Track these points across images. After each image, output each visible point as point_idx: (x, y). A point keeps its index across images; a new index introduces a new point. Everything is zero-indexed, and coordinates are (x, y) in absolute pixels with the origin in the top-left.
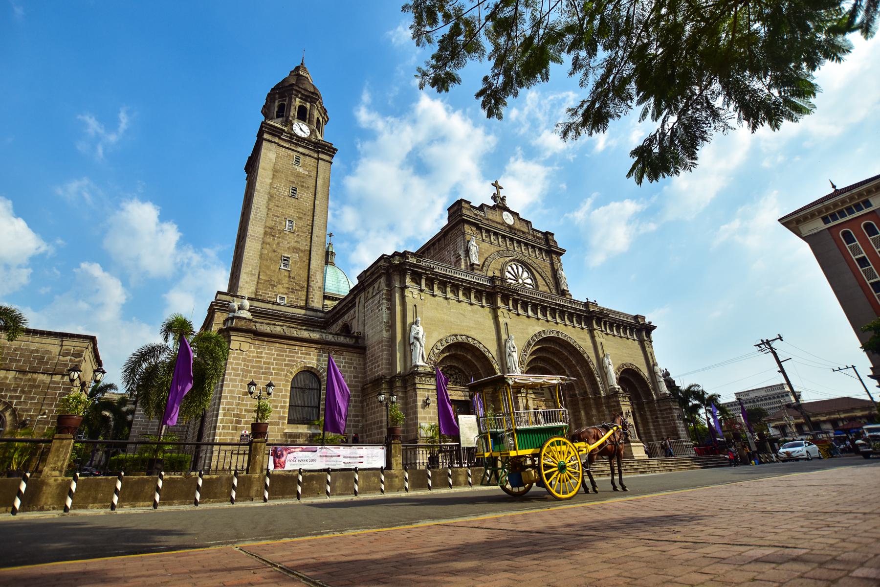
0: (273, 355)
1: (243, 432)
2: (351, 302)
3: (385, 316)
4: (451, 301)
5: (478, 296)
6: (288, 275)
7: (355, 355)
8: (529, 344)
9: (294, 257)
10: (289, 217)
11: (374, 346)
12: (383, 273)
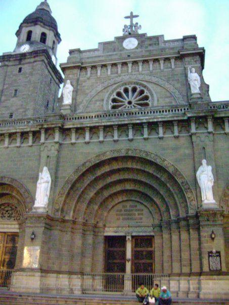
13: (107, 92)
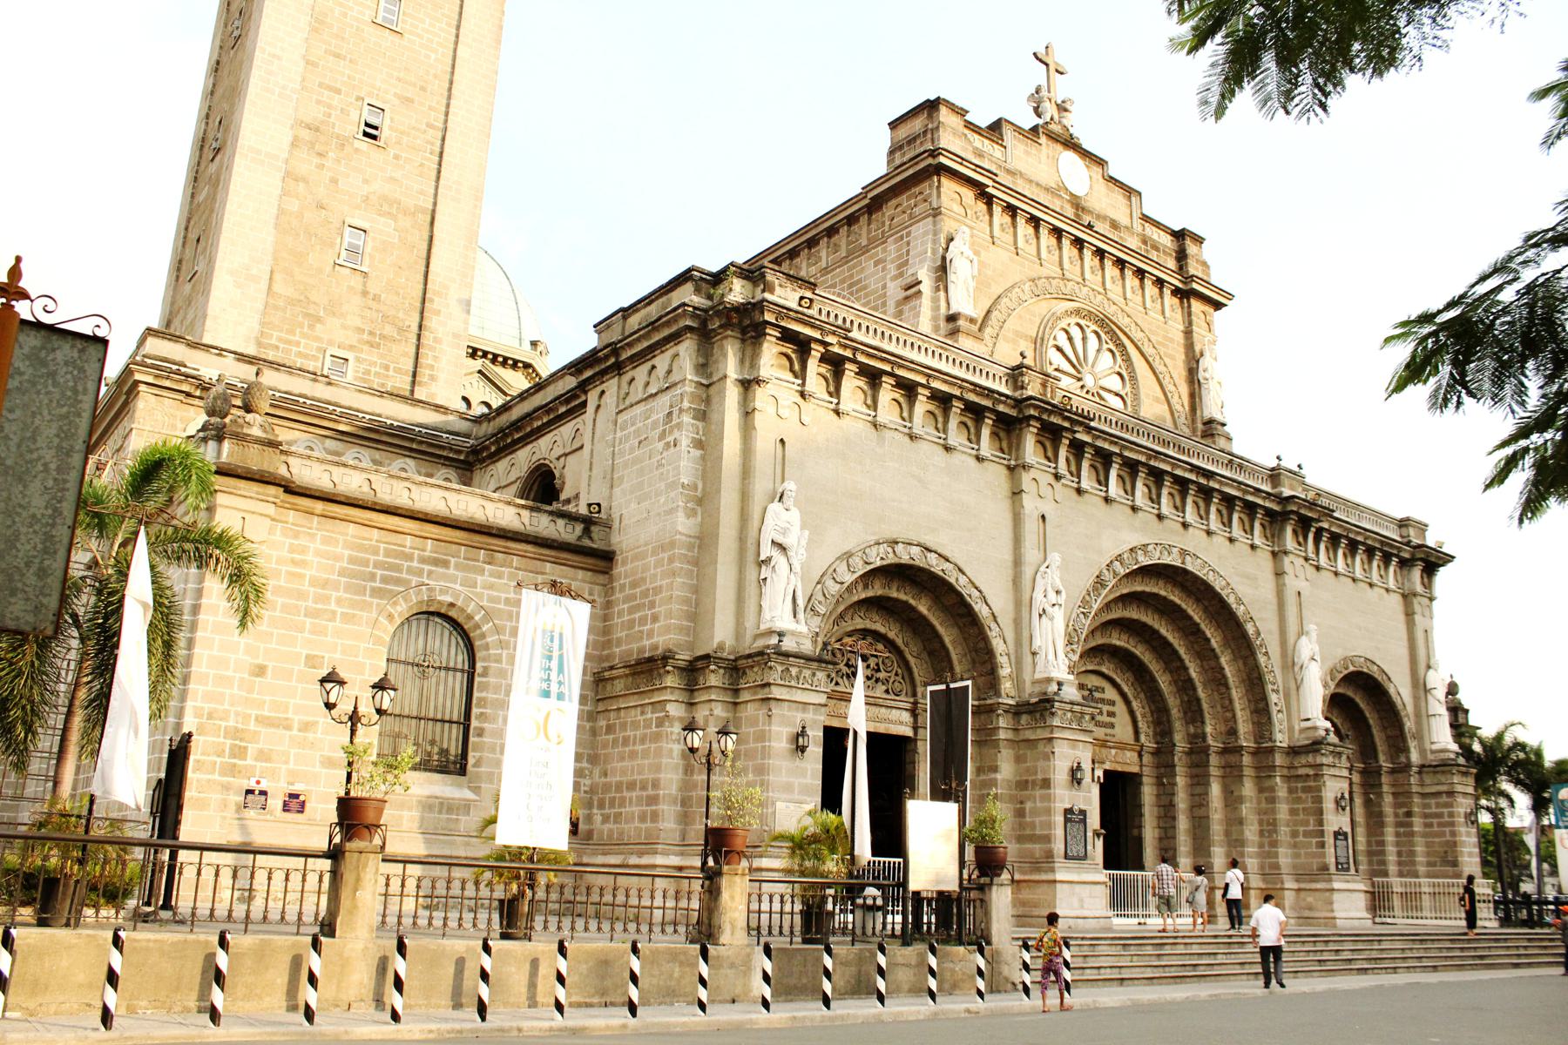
0: (337, 558)
2: (567, 401)
3: (686, 463)
5: (970, 423)
6: (360, 287)
7: (580, 574)
8: (1100, 582)
9: (382, 228)
10: (370, 94)
12: (689, 329)
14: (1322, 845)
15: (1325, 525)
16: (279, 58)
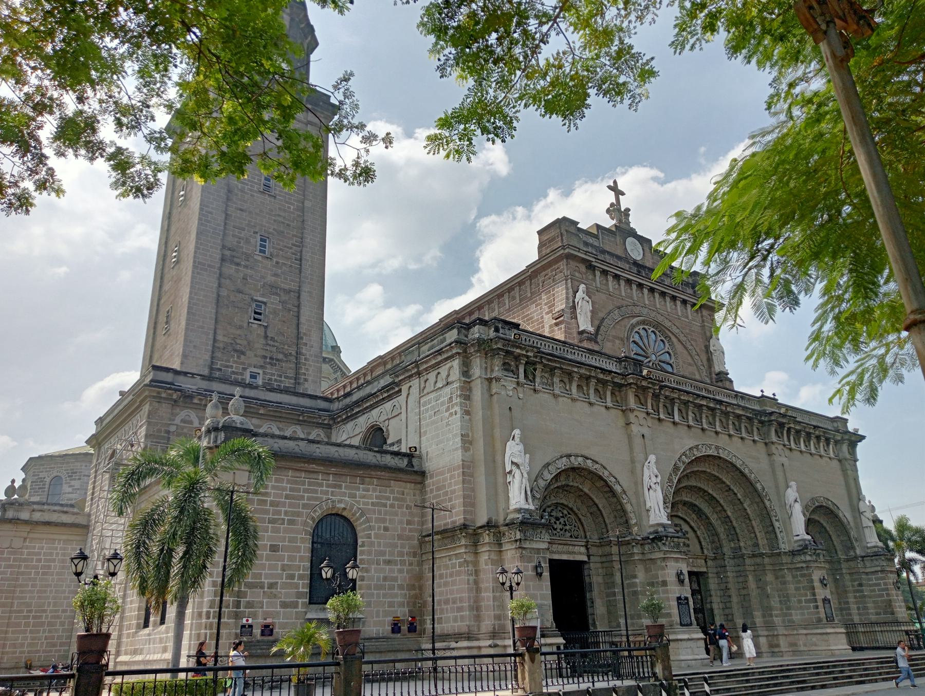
0: (284, 489)
1: (244, 621)
2: (388, 391)
4: (561, 399)
6: (263, 334)
7: (408, 485)
9: (273, 302)
11: (442, 473)
13: (625, 327)
14: (817, 607)
15: (792, 426)
16: (211, 213)
